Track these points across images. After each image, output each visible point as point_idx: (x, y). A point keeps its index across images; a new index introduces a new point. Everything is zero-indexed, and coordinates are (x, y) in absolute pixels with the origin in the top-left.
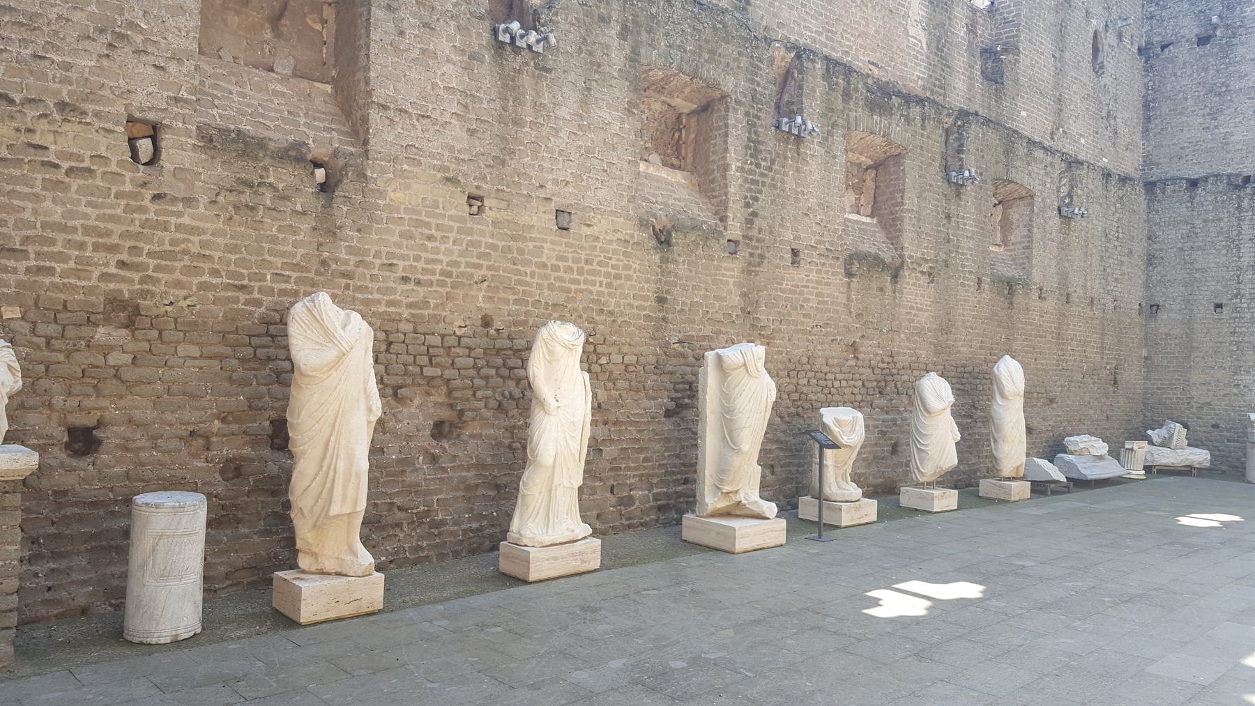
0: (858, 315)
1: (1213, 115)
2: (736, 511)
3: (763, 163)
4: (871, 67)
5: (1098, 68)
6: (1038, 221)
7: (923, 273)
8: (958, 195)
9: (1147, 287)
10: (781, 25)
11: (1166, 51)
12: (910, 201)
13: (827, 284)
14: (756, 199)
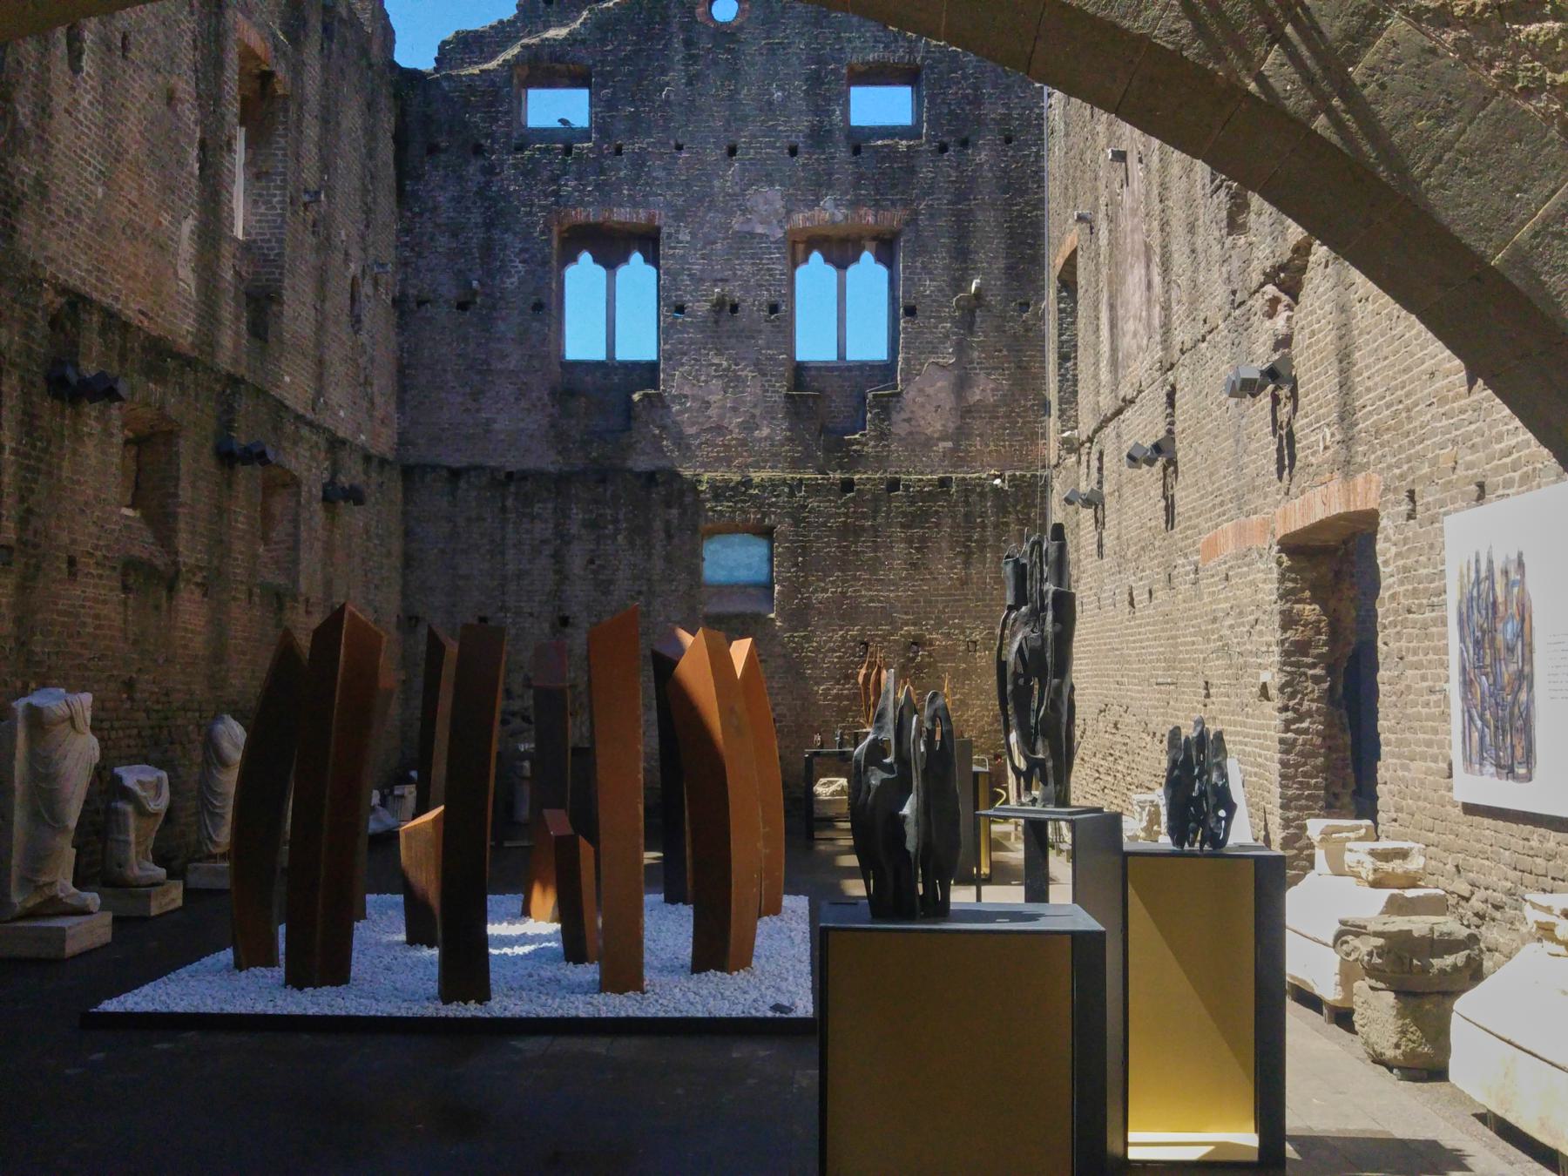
0: (135, 642)
1: (476, 395)
2: (55, 907)
3: (39, 444)
4: (142, 317)
5: (356, 321)
6: (305, 515)
7: (197, 584)
8: (230, 486)
9: (404, 594)
10: (50, 260)
11: (423, 308)
12: (185, 493)
13: (105, 602)
14: (32, 491)
